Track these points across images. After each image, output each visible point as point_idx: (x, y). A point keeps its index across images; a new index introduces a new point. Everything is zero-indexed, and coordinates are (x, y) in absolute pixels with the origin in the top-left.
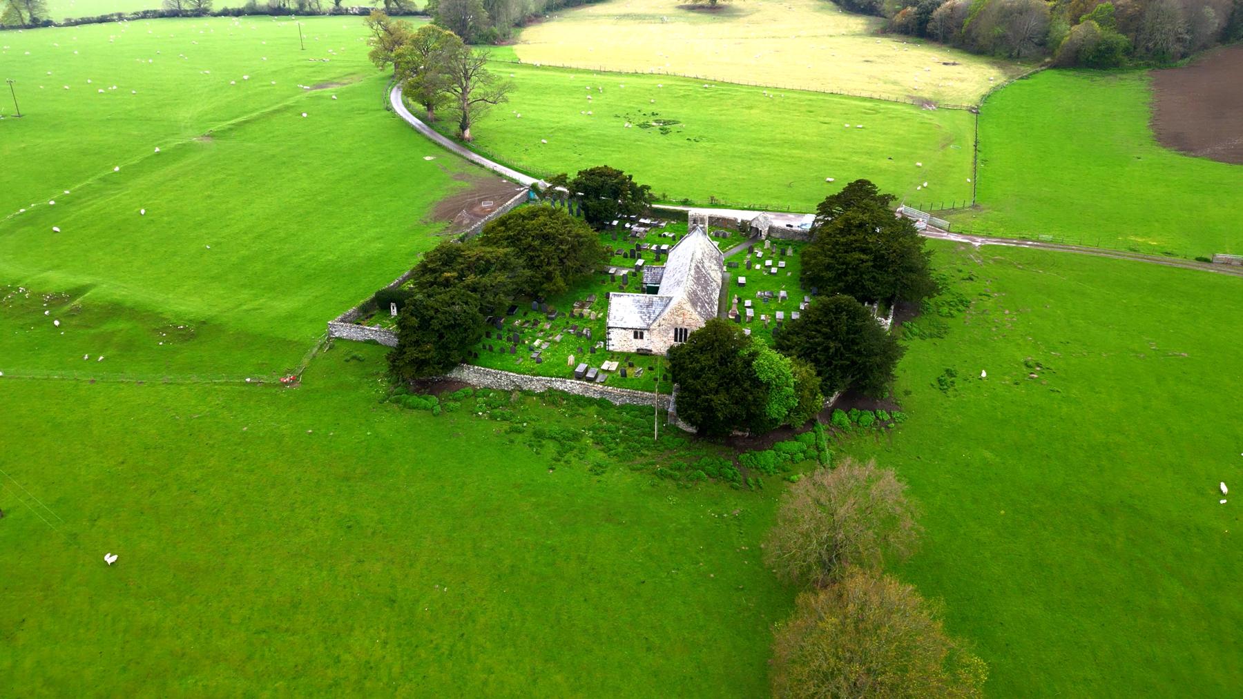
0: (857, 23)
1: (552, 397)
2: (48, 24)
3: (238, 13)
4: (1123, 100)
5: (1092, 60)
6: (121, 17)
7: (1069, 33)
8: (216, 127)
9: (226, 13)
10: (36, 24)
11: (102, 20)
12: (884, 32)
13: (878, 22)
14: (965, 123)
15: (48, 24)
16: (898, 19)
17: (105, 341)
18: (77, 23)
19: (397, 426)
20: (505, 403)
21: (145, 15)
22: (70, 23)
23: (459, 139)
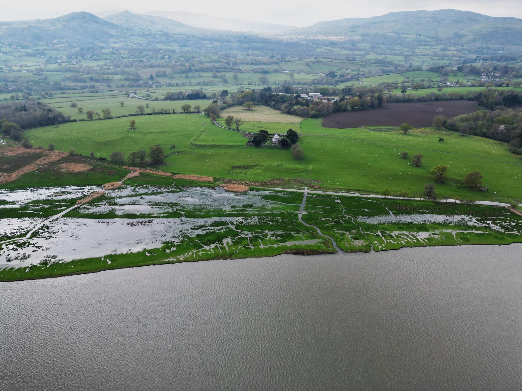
0: (278, 112)
1: (270, 146)
2: (112, 118)
3: (151, 114)
4: (319, 121)
5: (315, 116)
6: (125, 116)
7: (312, 112)
8: (201, 130)
9: (147, 114)
10: (109, 118)
11: (122, 117)
12: (283, 113)
13: (282, 112)
14: (299, 125)
15: (112, 118)
16: (285, 111)
17: (223, 148)
18: (118, 117)
19: (256, 150)
20: (266, 147)
21: (130, 115)
22: (116, 118)
23: (237, 130)
